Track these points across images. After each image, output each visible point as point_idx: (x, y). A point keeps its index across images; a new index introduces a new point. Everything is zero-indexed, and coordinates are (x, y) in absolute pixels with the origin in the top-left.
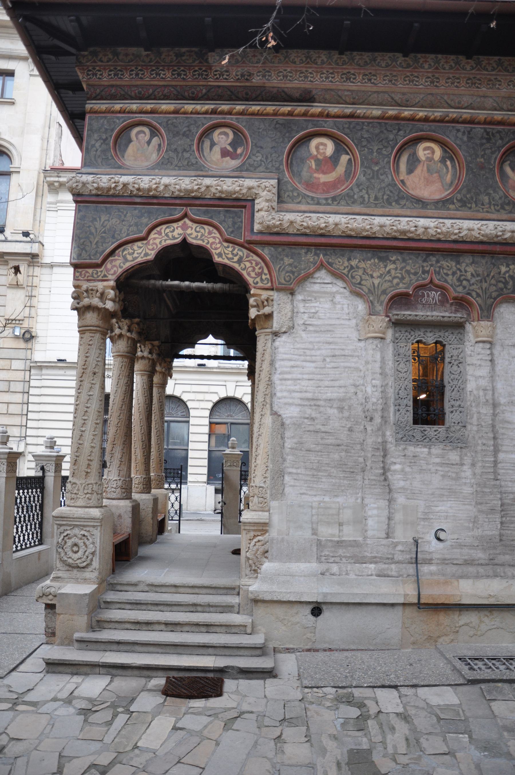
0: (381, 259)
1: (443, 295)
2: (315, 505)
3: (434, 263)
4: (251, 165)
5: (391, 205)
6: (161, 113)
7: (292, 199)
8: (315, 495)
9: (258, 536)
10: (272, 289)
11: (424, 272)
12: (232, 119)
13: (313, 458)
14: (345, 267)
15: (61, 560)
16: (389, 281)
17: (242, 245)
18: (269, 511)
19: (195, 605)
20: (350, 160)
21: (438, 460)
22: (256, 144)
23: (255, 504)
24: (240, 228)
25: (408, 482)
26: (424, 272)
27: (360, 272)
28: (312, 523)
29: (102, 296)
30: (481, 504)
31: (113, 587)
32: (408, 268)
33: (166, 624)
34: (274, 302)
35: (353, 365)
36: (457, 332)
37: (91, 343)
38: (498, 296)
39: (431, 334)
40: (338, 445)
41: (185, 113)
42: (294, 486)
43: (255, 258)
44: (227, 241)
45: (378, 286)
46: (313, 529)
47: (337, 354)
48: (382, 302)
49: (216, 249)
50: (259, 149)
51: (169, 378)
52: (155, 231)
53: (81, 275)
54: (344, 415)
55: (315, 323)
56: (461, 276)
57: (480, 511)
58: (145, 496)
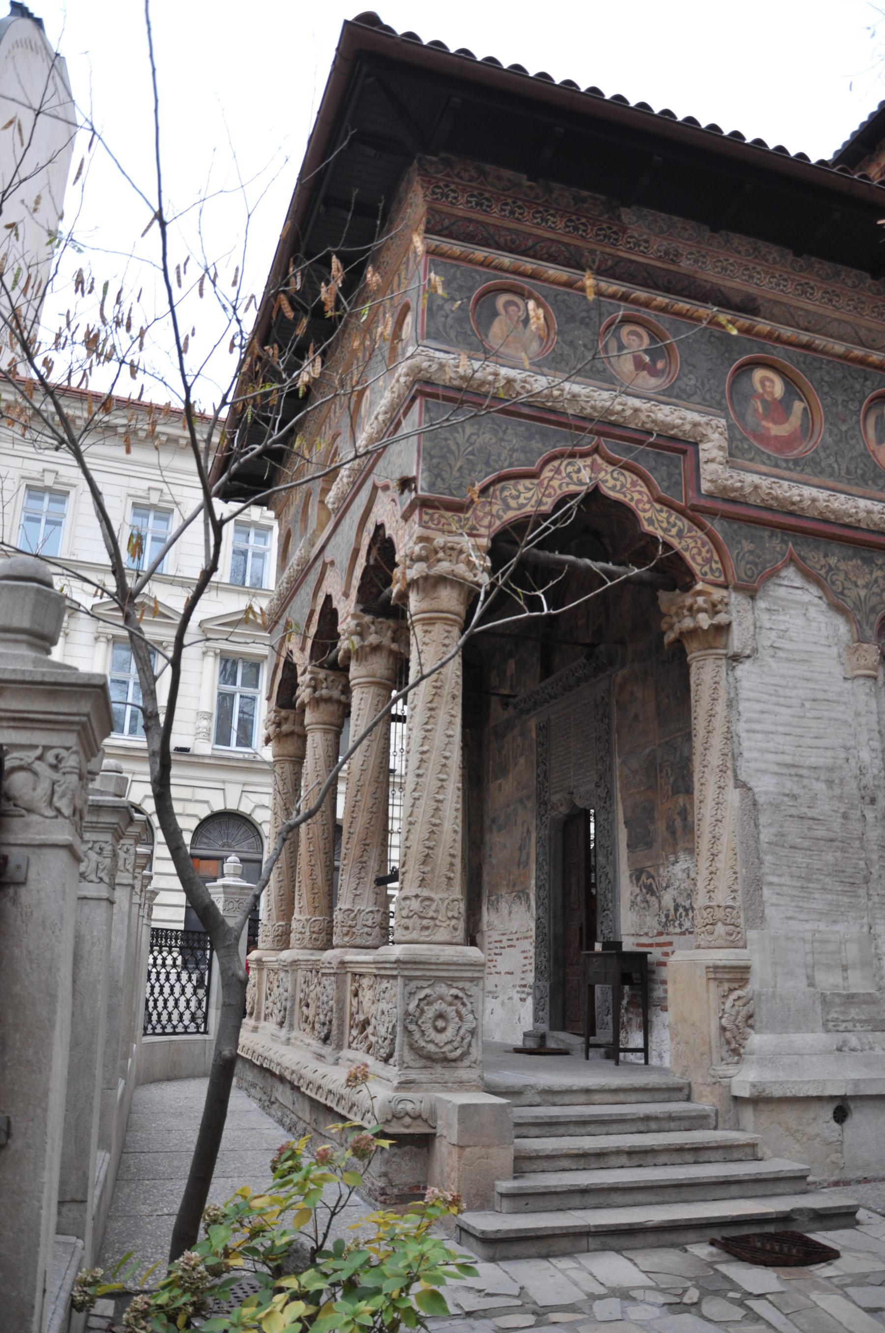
0: (865, 561)
2: (808, 936)
4: (683, 391)
6: (545, 280)
8: (807, 921)
9: (735, 989)
10: (726, 587)
13: (800, 860)
15: (411, 1047)
16: (878, 594)
17: (681, 512)
19: (647, 1118)
20: (805, 409)
23: (720, 936)
24: (678, 483)
27: (841, 577)
28: (806, 966)
35: (840, 716)
37: (447, 642)
40: (831, 840)
43: (700, 533)
44: (660, 500)
49: (644, 511)
53: (432, 519)
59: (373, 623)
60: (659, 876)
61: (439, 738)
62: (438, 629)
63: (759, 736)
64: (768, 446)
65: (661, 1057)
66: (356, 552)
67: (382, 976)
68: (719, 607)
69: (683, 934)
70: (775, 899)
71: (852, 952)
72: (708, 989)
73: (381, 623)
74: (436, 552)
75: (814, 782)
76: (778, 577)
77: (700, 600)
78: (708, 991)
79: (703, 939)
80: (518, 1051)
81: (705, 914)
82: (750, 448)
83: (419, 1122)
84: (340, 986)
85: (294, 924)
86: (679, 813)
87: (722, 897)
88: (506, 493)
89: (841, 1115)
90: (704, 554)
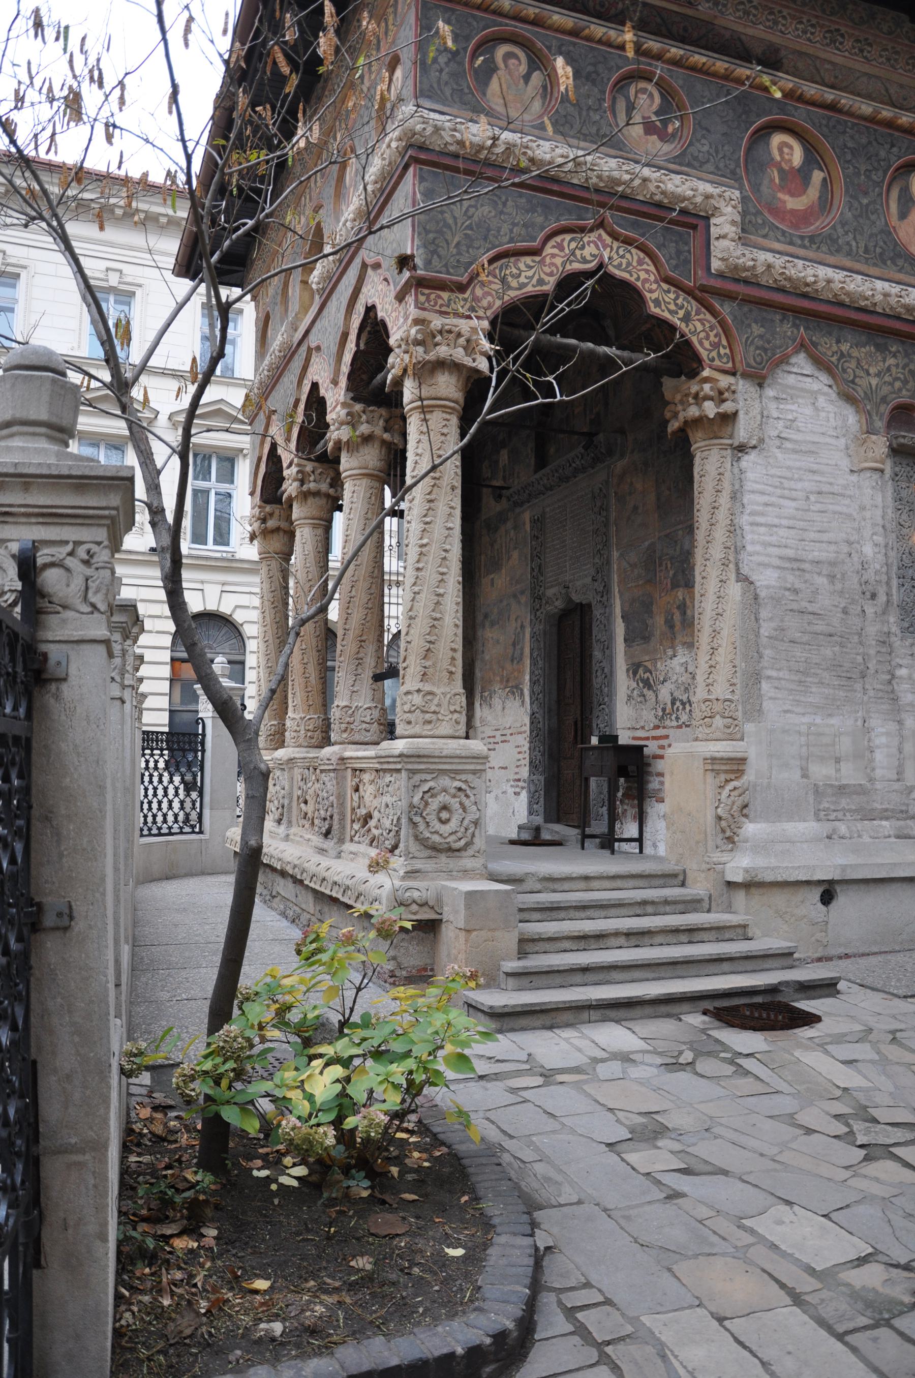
0: (878, 347)
2: (804, 729)
4: (696, 158)
5: (885, 264)
10: (734, 374)
13: (798, 654)
15: (416, 838)
17: (689, 292)
19: (644, 903)
22: (699, 123)
24: (687, 262)
27: (853, 364)
28: (801, 758)
29: (470, 347)
33: (628, 934)
35: (845, 510)
37: (445, 431)
42: (775, 699)
43: (709, 316)
44: (667, 280)
47: (824, 489)
49: (651, 291)
53: (428, 300)
59: (364, 412)
60: (656, 670)
61: (438, 530)
62: (436, 418)
63: (762, 530)
64: (783, 220)
65: (655, 846)
66: (345, 336)
67: (385, 771)
68: (726, 395)
69: (680, 727)
70: (772, 693)
71: (845, 745)
72: (705, 780)
73: (372, 411)
74: (434, 337)
75: (815, 576)
76: (788, 363)
77: (707, 387)
78: (705, 783)
79: (701, 732)
80: (513, 842)
81: (703, 707)
82: (764, 223)
83: (426, 909)
84: (340, 782)
85: (288, 723)
86: (678, 608)
87: (720, 690)
89: (827, 898)
90: (712, 338)
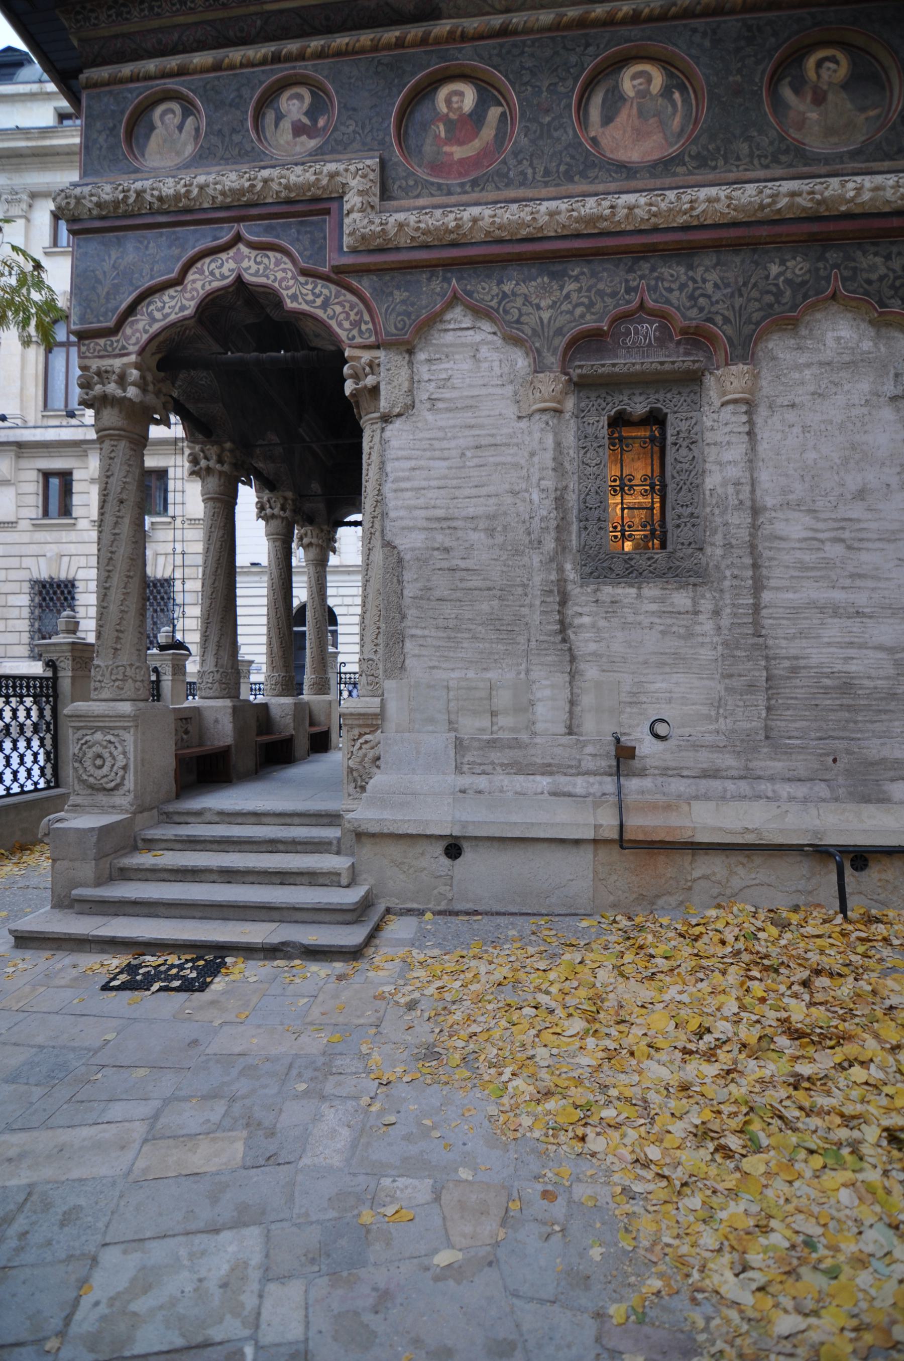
0: (553, 276)
1: (663, 328)
3: (647, 272)
7: (406, 191)
10: (378, 347)
11: (628, 290)
12: (306, 68)
14: (493, 297)
16: (568, 312)
17: (326, 278)
18: (383, 695)
20: (503, 114)
21: (654, 607)
22: (345, 107)
25: (603, 644)
26: (628, 290)
27: (519, 301)
29: (122, 381)
30: (730, 676)
31: (169, 818)
32: (601, 286)
34: (382, 368)
35: (509, 459)
36: (688, 390)
37: (112, 455)
38: (763, 319)
39: (642, 398)
40: (489, 589)
41: (232, 67)
44: (305, 273)
45: (549, 322)
46: (450, 722)
47: (483, 443)
48: (556, 349)
49: (288, 288)
50: (351, 112)
51: (331, 553)
52: (194, 269)
53: (88, 350)
54: (496, 542)
55: (448, 395)
56: (695, 289)
57: (726, 689)
58: (288, 700)
75: (471, 533)
82: (416, 182)
88: (152, 307)
90: (352, 317)
